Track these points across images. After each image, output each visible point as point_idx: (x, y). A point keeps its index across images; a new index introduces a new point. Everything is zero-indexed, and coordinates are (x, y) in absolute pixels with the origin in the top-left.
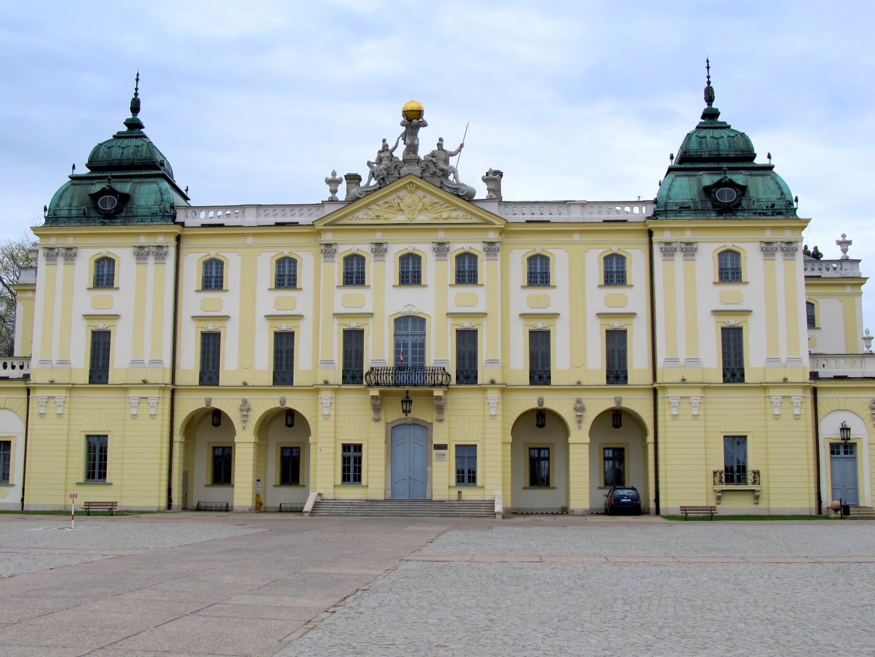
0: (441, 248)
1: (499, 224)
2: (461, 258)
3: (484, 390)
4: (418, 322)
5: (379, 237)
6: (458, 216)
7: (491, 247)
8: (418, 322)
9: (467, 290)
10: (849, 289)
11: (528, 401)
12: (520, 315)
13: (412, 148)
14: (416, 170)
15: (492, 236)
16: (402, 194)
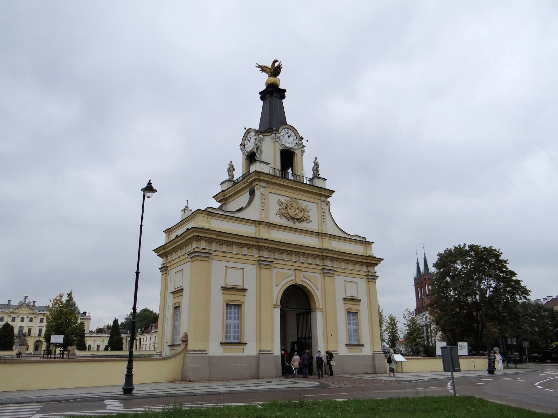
0: (28, 317)
1: (37, 314)
2: (30, 318)
3: (31, 337)
4: (23, 327)
5: (18, 315)
6: (31, 312)
7: (35, 317)
8: (23, 327)
9: (31, 323)
10: (89, 320)
11: (37, 339)
12: (39, 327)
13: (25, 301)
14: (26, 305)
15: (36, 315)
16: (23, 308)
